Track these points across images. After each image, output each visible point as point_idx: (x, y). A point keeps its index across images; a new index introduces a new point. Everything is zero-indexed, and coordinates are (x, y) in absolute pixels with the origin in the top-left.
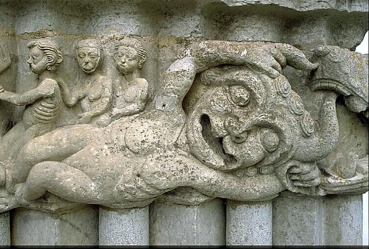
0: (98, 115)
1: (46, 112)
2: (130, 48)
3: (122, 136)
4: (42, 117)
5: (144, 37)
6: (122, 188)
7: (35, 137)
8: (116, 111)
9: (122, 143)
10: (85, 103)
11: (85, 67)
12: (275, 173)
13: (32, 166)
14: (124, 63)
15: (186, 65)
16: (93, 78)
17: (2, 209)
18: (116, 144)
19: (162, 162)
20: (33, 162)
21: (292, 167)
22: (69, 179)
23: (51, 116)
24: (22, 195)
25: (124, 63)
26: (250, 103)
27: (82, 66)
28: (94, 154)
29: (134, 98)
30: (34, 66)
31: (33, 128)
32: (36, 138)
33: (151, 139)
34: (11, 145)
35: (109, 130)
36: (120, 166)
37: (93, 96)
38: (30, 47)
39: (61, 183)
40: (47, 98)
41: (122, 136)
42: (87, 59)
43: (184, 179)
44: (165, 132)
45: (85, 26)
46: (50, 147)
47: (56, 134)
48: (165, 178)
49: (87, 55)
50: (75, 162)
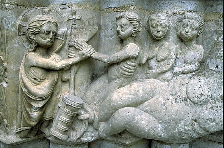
0: (164, 72)
1: (130, 69)
2: (193, 20)
3: (184, 89)
4: (126, 73)
5: (199, 13)
6: (182, 130)
7: (119, 88)
8: (177, 69)
9: (184, 95)
10: (153, 63)
11: (156, 35)
13: (117, 110)
14: (188, 32)
16: (161, 43)
17: (89, 141)
18: (179, 96)
19: (214, 111)
20: (118, 107)
22: (143, 122)
23: (132, 72)
24: (104, 130)
25: (188, 32)
27: (154, 34)
28: (162, 103)
29: (193, 61)
30: (122, 33)
31: (118, 81)
32: (119, 89)
33: (206, 93)
34: (96, 92)
35: (172, 84)
36: (182, 113)
37: (161, 57)
38: (118, 19)
39: (138, 125)
40: (132, 58)
41: (184, 89)
42: (159, 28)
44: (215, 87)
45: (152, 3)
46: (130, 96)
47: (134, 86)
48: (215, 124)
49: (159, 26)
50: (147, 108)
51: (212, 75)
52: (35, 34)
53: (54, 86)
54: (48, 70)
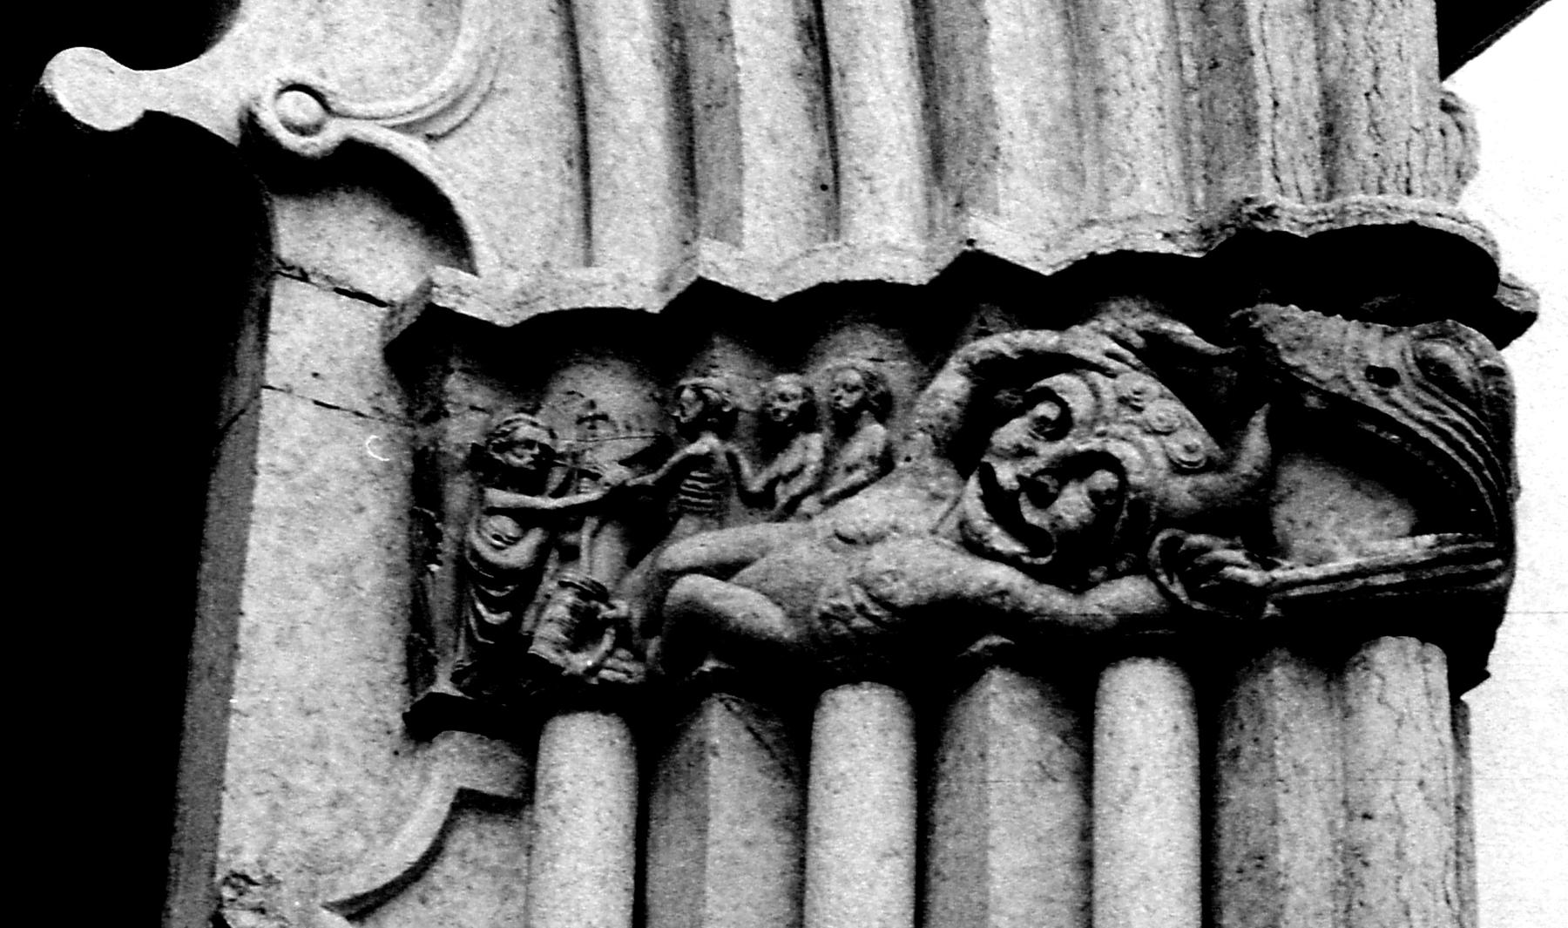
8: (830, 492)
10: (779, 489)
12: (1141, 568)
15: (951, 384)
21: (1171, 545)
26: (1062, 426)
30: (683, 420)
43: (947, 584)
51: (898, 480)
52: (501, 449)
53: (542, 553)
54: (526, 519)
